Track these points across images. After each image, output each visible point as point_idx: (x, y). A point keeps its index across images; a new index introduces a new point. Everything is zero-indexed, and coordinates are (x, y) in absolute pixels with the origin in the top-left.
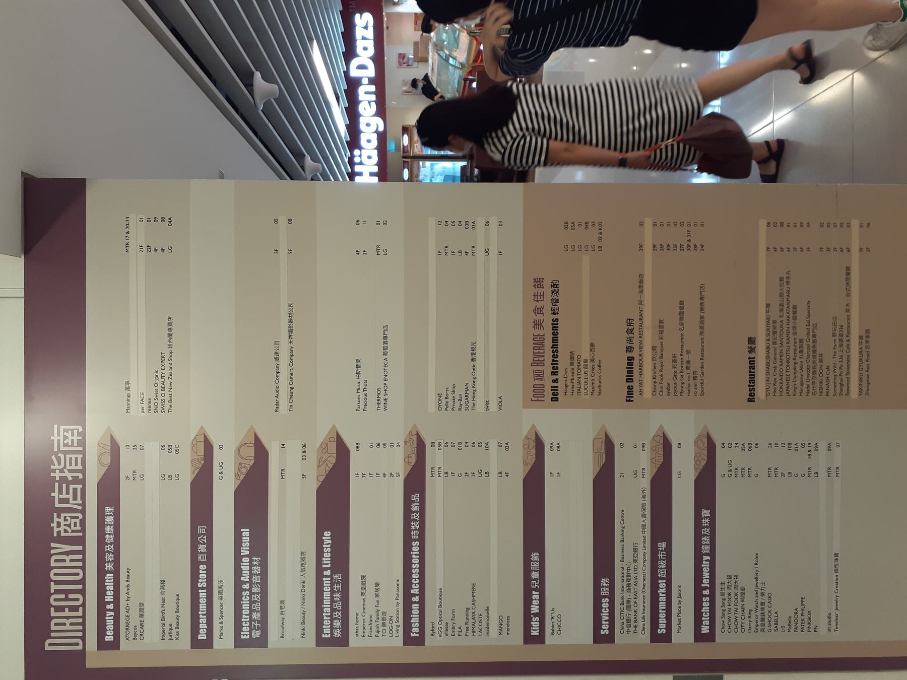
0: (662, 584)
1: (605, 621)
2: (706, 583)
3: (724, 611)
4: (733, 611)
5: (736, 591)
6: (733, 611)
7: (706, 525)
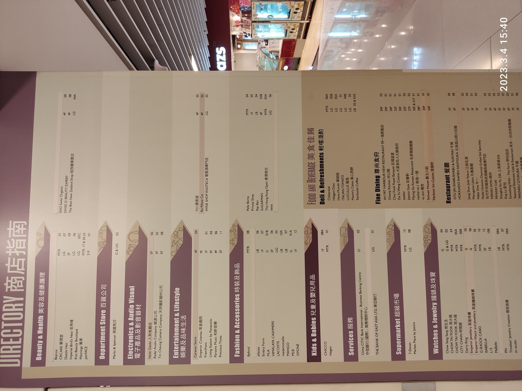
0: (398, 321)
1: (351, 346)
2: (435, 320)
3: (448, 338)
4: (454, 338)
5: (456, 325)
6: (454, 338)
7: (433, 282)
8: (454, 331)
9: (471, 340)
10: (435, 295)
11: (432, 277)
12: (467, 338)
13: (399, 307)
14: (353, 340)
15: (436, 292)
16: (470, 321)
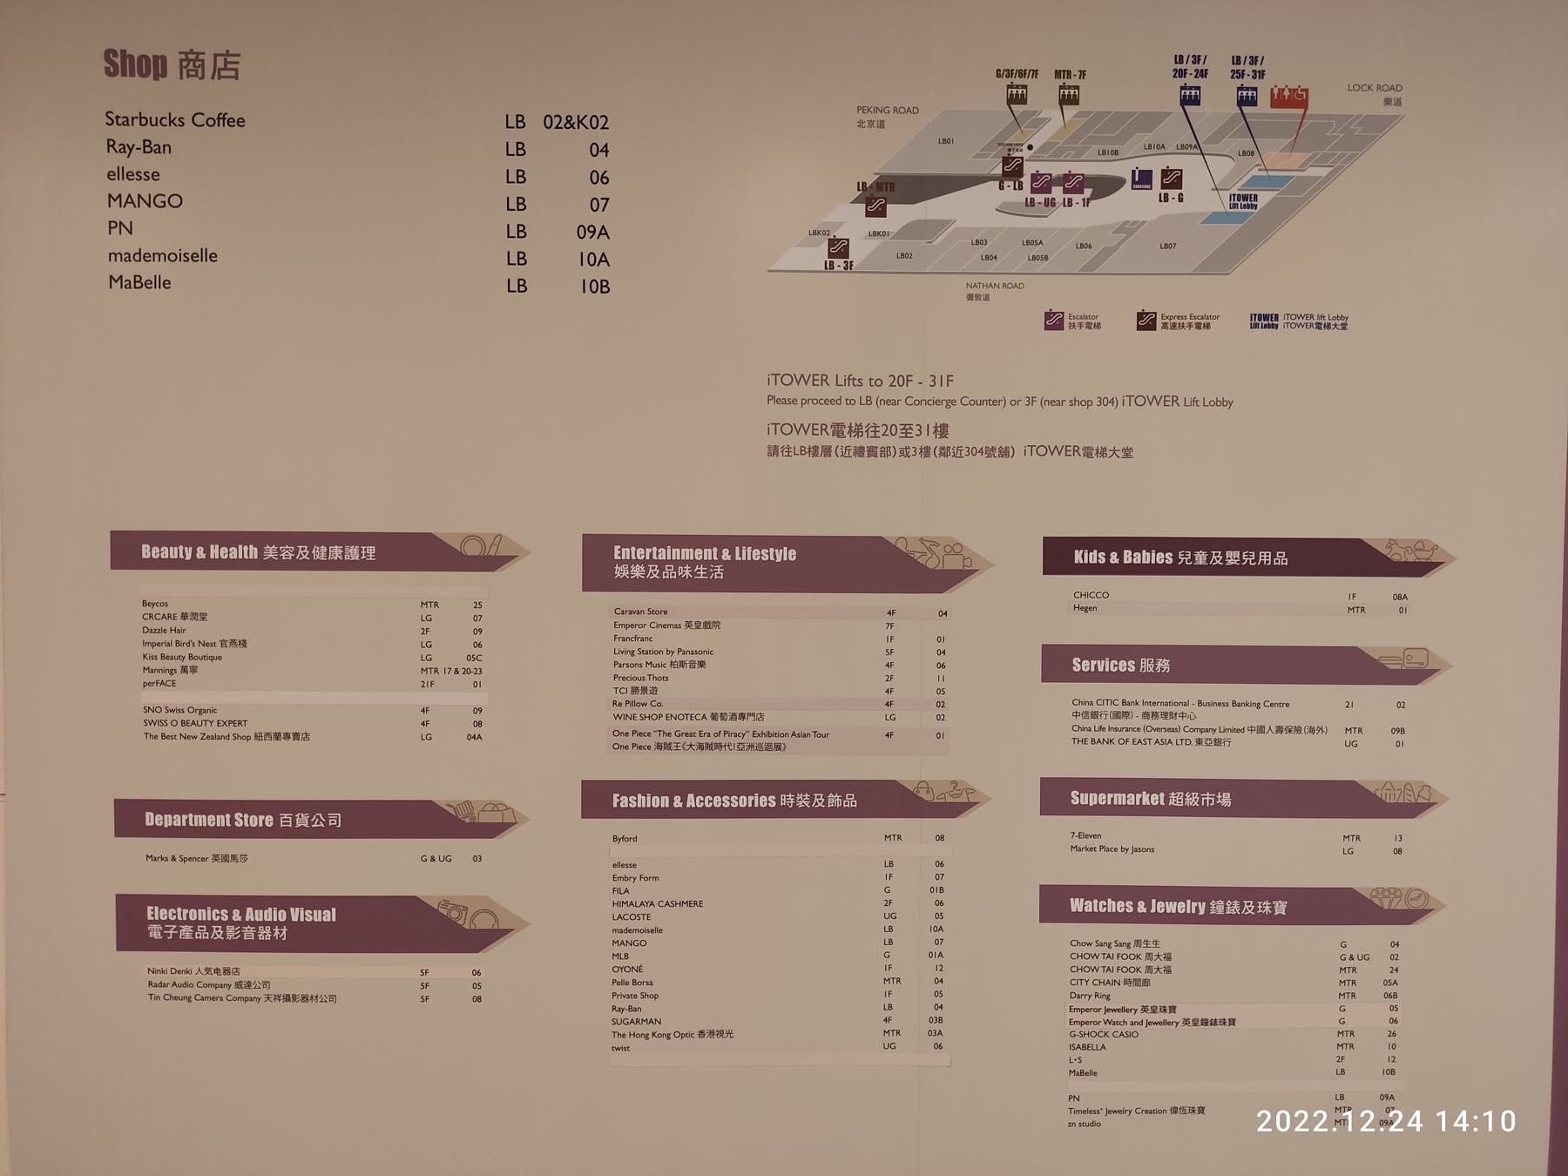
0: (1157, 799)
1: (1096, 666)
2: (1159, 907)
3: (1109, 946)
4: (1108, 963)
5: (1143, 970)
6: (1108, 963)
7: (1260, 907)
8: (1129, 963)
9: (1102, 1011)
10: (1225, 911)
11: (1273, 905)
12: (1108, 998)
13: (1196, 803)
14: (1112, 670)
15: (1234, 913)
16: (1154, 1010)
